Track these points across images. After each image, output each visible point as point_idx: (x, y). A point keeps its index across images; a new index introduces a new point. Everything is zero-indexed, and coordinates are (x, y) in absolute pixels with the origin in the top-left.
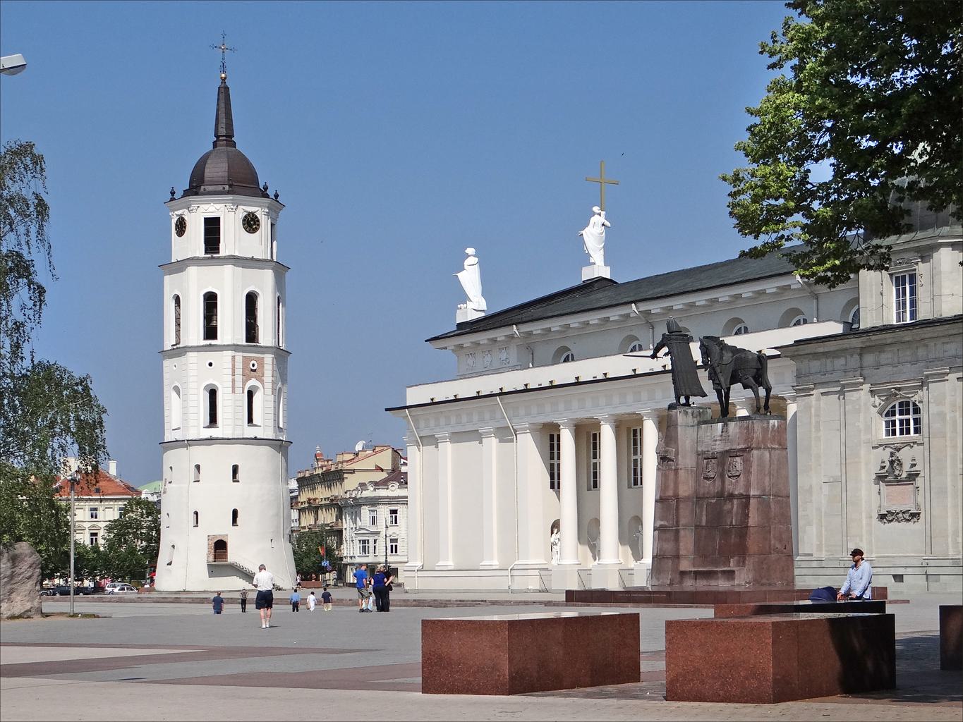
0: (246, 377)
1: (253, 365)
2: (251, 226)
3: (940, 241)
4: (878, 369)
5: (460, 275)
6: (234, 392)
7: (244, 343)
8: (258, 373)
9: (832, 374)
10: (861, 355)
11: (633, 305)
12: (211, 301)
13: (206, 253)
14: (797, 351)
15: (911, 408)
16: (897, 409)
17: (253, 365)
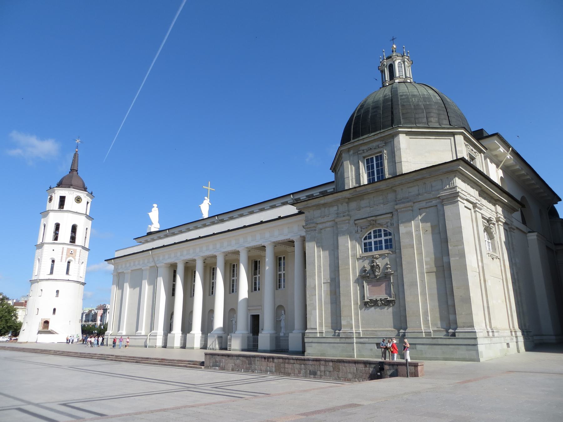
0: (68, 256)
1: (72, 252)
2: (78, 200)
3: (400, 130)
4: (360, 210)
5: (150, 214)
6: (61, 261)
7: (69, 243)
8: (74, 255)
9: (329, 216)
10: (348, 203)
11: (216, 217)
12: (57, 226)
13: (59, 209)
14: (307, 205)
15: (383, 233)
16: (372, 235)
17: (72, 252)
